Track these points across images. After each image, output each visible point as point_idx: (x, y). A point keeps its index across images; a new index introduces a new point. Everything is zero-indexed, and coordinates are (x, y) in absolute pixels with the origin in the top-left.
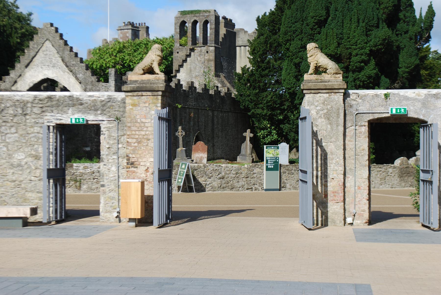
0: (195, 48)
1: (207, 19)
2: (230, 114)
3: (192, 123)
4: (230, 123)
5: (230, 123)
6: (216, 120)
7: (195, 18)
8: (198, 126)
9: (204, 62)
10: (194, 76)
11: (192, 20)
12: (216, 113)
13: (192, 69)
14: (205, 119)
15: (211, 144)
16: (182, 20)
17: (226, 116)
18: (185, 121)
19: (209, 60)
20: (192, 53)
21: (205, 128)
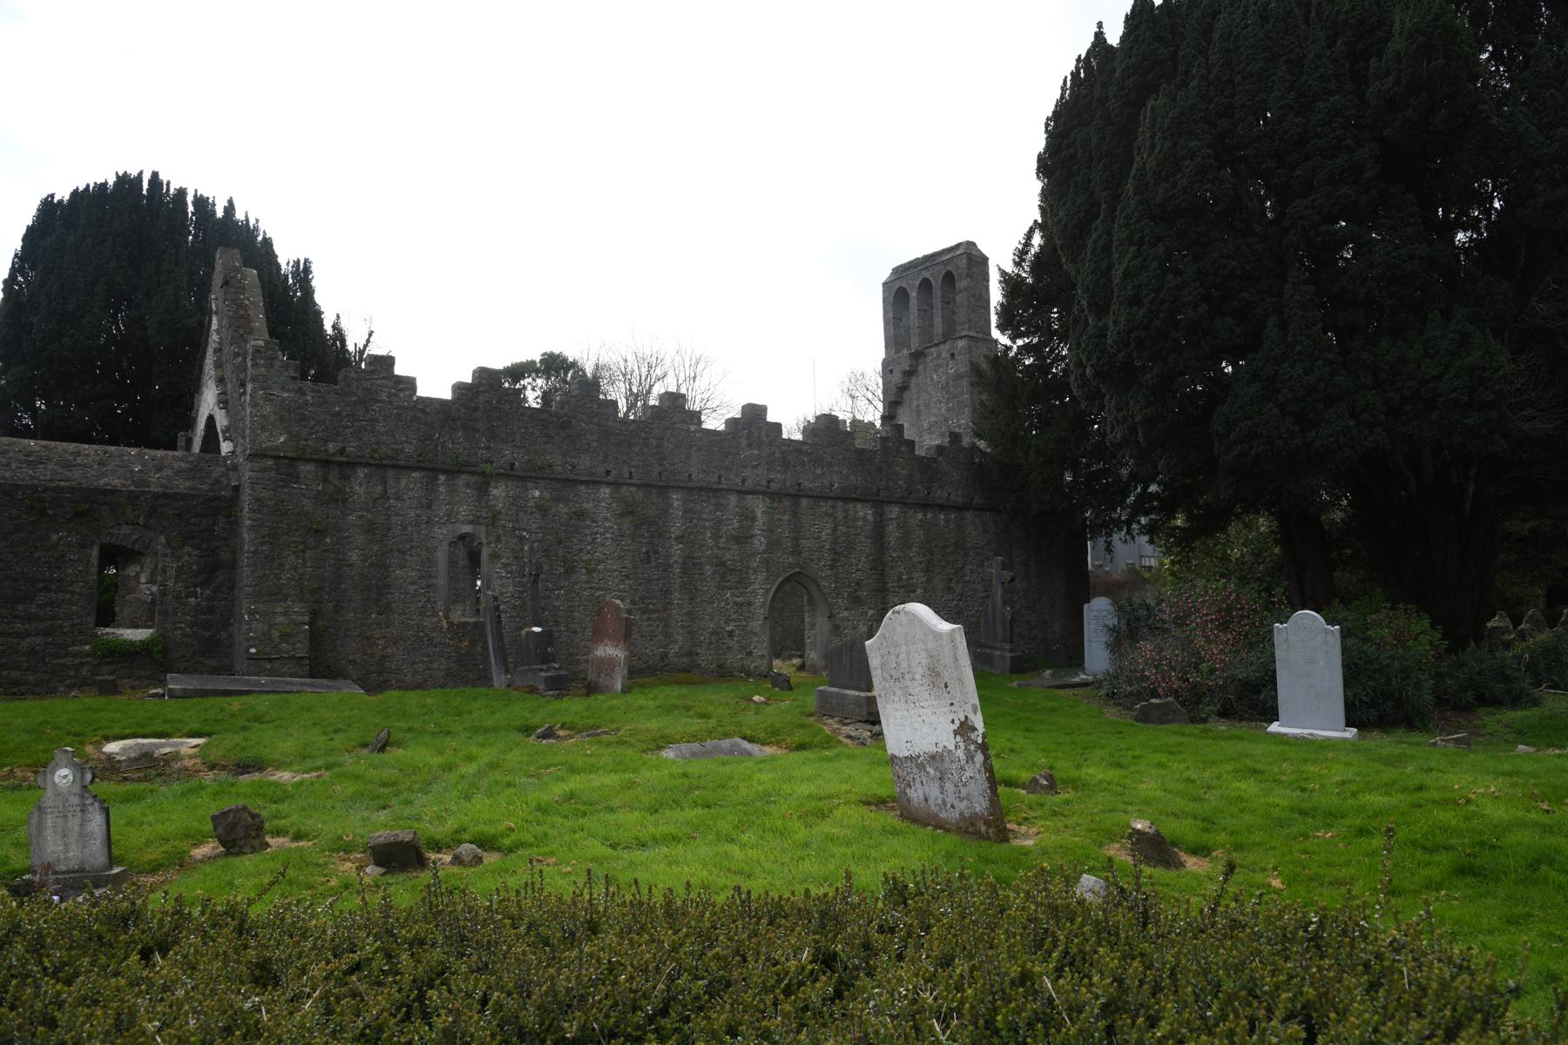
0: (926, 351)
1: (949, 269)
2: (968, 515)
3: (759, 543)
4: (968, 545)
5: (968, 545)
6: (893, 533)
7: (926, 274)
8: (796, 551)
9: (947, 384)
10: (926, 426)
11: (917, 283)
12: (894, 511)
13: (922, 408)
14: (835, 529)
15: (871, 612)
16: (898, 285)
17: (947, 521)
18: (716, 537)
19: (958, 377)
20: (921, 368)
21: (833, 560)
